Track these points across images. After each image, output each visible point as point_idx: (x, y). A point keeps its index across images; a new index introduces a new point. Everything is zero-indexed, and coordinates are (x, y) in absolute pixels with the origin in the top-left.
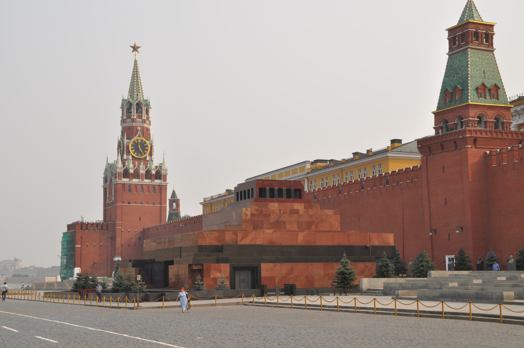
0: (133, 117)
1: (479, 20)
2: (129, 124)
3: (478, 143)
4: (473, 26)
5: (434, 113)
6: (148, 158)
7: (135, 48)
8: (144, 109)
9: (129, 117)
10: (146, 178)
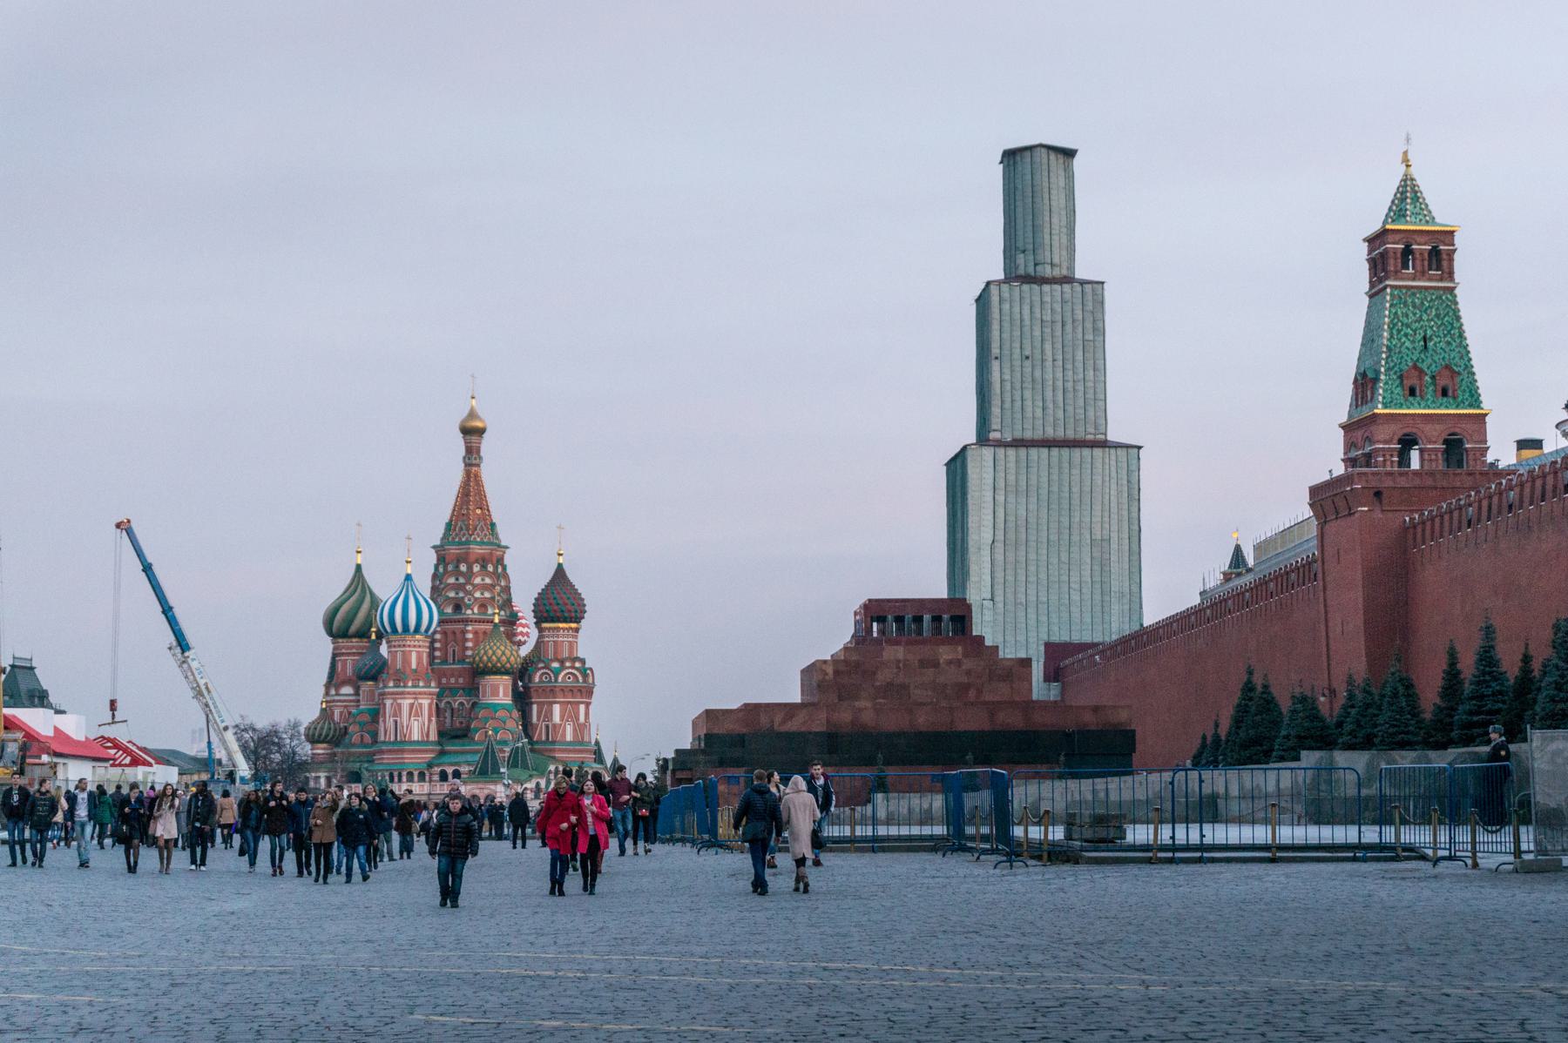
1: (1421, 220)
5: (1344, 427)
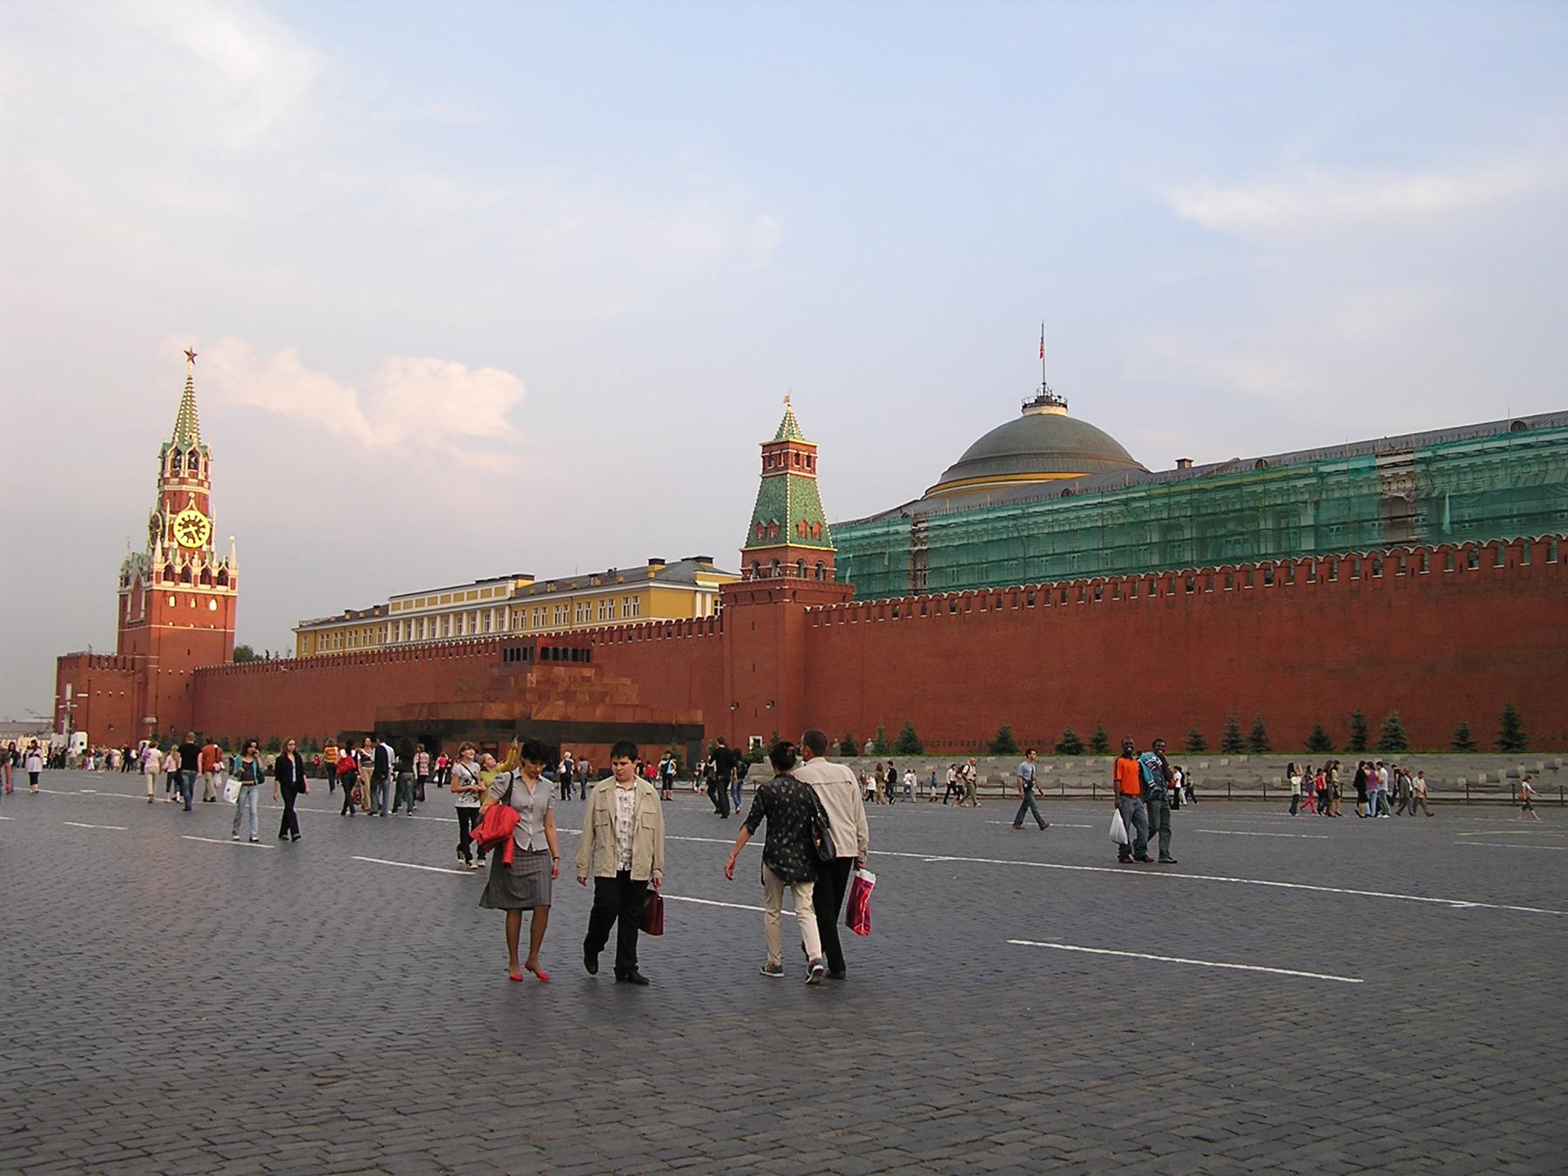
0: (181, 475)
2: (173, 486)
3: (797, 597)
4: (794, 445)
6: (205, 548)
7: (191, 356)
8: (202, 460)
9: (175, 474)
10: (201, 583)
